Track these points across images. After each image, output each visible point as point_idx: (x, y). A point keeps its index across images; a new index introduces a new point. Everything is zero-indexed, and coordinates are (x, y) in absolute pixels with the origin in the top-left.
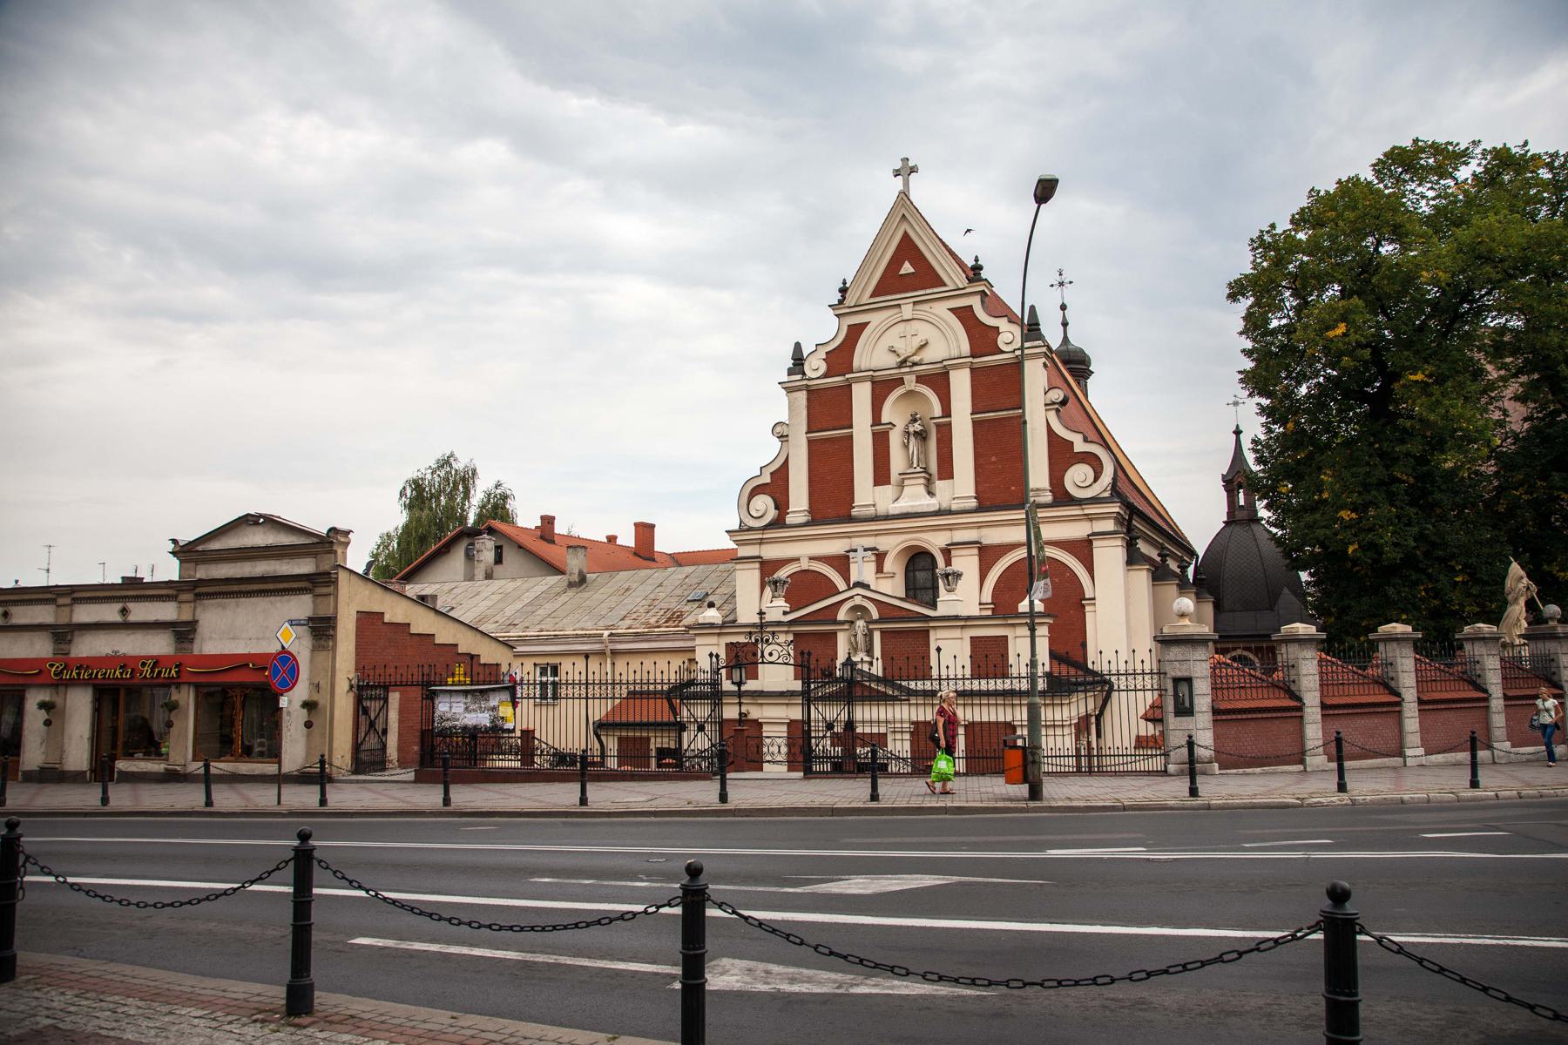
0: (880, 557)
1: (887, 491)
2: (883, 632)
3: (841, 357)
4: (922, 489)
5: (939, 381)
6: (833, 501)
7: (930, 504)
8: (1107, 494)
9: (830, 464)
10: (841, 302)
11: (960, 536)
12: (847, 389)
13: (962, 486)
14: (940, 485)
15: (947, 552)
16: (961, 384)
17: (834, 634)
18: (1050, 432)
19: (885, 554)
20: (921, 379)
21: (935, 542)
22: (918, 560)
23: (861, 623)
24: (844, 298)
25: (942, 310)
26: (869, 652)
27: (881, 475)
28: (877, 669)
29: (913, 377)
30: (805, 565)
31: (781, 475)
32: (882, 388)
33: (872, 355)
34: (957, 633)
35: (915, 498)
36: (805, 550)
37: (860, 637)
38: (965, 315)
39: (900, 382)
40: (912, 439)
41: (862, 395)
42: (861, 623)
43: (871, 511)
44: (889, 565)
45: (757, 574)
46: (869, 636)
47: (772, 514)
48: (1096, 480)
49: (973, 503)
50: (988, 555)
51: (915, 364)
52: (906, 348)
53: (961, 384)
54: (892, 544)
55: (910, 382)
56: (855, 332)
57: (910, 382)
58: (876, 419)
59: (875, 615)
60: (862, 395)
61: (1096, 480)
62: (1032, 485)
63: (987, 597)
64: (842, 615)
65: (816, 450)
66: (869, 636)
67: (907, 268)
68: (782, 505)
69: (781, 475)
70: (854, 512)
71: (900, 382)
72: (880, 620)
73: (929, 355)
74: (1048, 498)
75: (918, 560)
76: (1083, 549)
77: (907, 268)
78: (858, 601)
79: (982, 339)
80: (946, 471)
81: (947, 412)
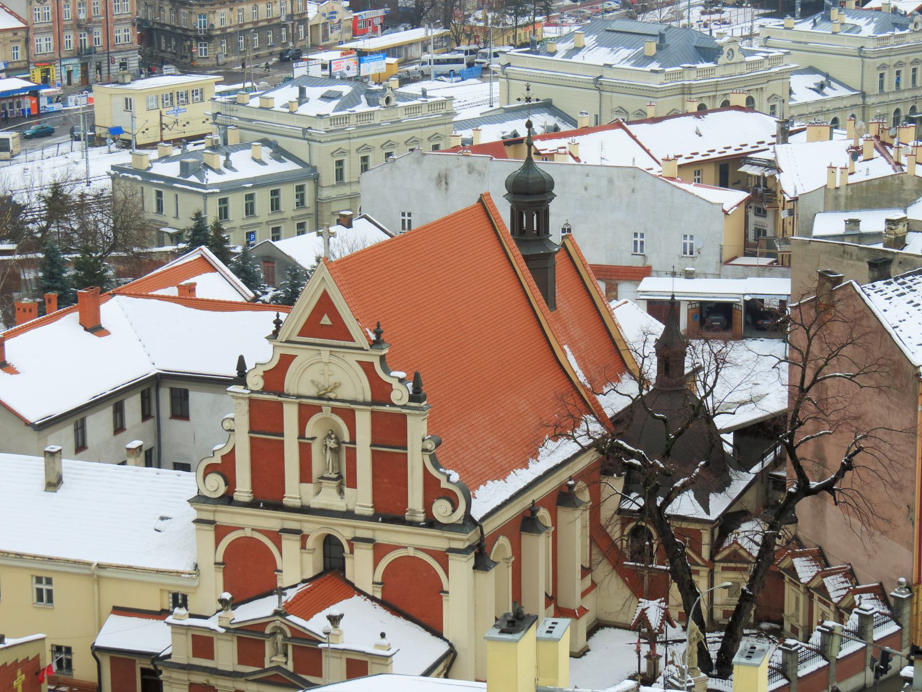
0: (304, 539)
1: (309, 488)
2: (293, 646)
3: (275, 378)
4: (334, 492)
5: (349, 417)
6: (268, 496)
7: (338, 504)
8: (461, 522)
9: (267, 458)
10: (275, 334)
11: (360, 534)
13: (361, 497)
14: (347, 490)
16: (363, 420)
17: (263, 642)
18: (425, 470)
19: (307, 536)
20: (335, 410)
21: (344, 531)
22: (330, 544)
24: (278, 327)
26: (286, 655)
27: (305, 476)
28: (290, 667)
29: (330, 409)
30: (248, 533)
31: (229, 458)
32: (306, 413)
33: (298, 381)
34: (339, 655)
35: (329, 498)
37: (279, 645)
38: (368, 368)
40: (329, 452)
41: (290, 415)
44: (310, 543)
47: (222, 490)
48: (454, 511)
49: (370, 512)
50: (380, 551)
51: (330, 399)
53: (363, 420)
55: (327, 410)
56: (285, 361)
57: (327, 410)
58: (302, 435)
59: (289, 635)
60: (290, 415)
61: (454, 511)
62: (410, 505)
63: (379, 578)
64: (268, 631)
65: (255, 446)
66: (286, 646)
67: (326, 320)
68: (230, 482)
69: (229, 458)
70: (286, 501)
71: (319, 409)
72: (293, 638)
74: (421, 517)
75: (330, 544)
76: (442, 557)
77: (326, 320)
78: (278, 623)
79: (381, 393)
81: (353, 441)
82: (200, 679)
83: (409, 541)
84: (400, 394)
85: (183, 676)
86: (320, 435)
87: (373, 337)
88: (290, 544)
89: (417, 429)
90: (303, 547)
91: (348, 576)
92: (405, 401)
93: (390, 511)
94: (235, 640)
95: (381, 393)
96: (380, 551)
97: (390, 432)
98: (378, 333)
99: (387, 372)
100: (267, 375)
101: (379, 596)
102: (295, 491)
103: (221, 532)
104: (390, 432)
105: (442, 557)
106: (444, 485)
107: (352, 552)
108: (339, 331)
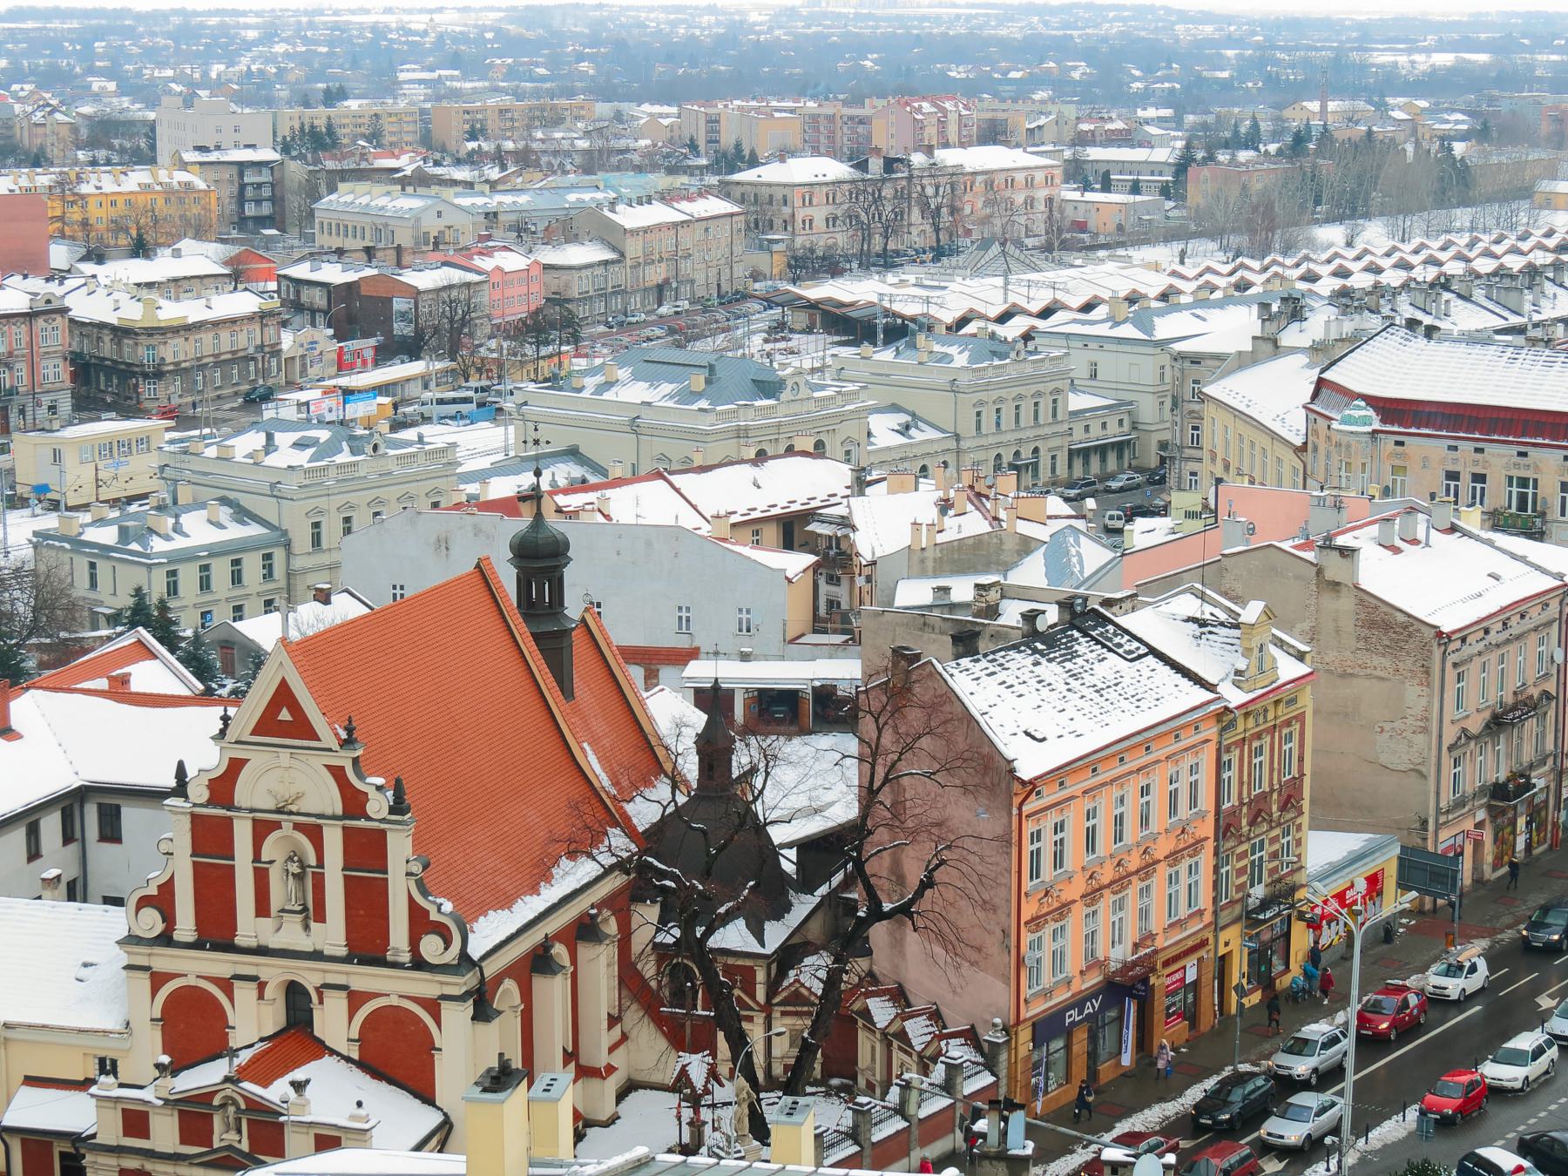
0: (262, 986)
3: (223, 787)
4: (299, 928)
5: (315, 834)
6: (216, 932)
7: (304, 943)
10: (223, 733)
11: (331, 979)
12: (229, 822)
13: (332, 934)
14: (313, 925)
15: (319, 990)
20: (297, 827)
21: (310, 976)
22: (294, 992)
23: (231, 1109)
24: (226, 725)
25: (318, 761)
26: (239, 1131)
27: (262, 909)
28: (245, 1146)
31: (167, 888)
32: (262, 830)
33: (251, 792)
35: (291, 935)
36: (197, 968)
38: (337, 773)
39: (277, 825)
42: (231, 1109)
43: (253, 943)
44: (269, 992)
45: (147, 983)
46: (238, 1121)
47: (159, 927)
48: (446, 949)
49: (343, 952)
50: (356, 999)
51: (291, 813)
52: (286, 792)
54: (275, 973)
55: (287, 827)
56: (236, 766)
57: (287, 827)
58: (257, 857)
59: (243, 1106)
61: (446, 949)
62: (393, 943)
64: (216, 1101)
66: (238, 1121)
67: (285, 715)
68: (169, 918)
69: (167, 888)
70: (239, 941)
73: (306, 805)
74: (406, 958)
75: (294, 992)
76: (433, 1006)
77: (285, 715)
78: (228, 1092)
79: (354, 803)
80: (320, 917)
81: (320, 864)
82: (132, 1163)
83: (393, 987)
84: (378, 805)
85: (112, 1161)
86: (280, 860)
87: (344, 735)
88: (245, 993)
89: (400, 848)
90: (261, 997)
91: (317, 1033)
92: (384, 813)
93: (367, 946)
94: (176, 1114)
95: (354, 803)
96: (356, 999)
97: (366, 851)
98: (350, 730)
99: (361, 777)
100: (213, 785)
101: (355, 1056)
102: (249, 928)
103: (158, 980)
104: (366, 851)
105: (433, 1006)
106: (434, 916)
107: (321, 1002)
108: (302, 728)
